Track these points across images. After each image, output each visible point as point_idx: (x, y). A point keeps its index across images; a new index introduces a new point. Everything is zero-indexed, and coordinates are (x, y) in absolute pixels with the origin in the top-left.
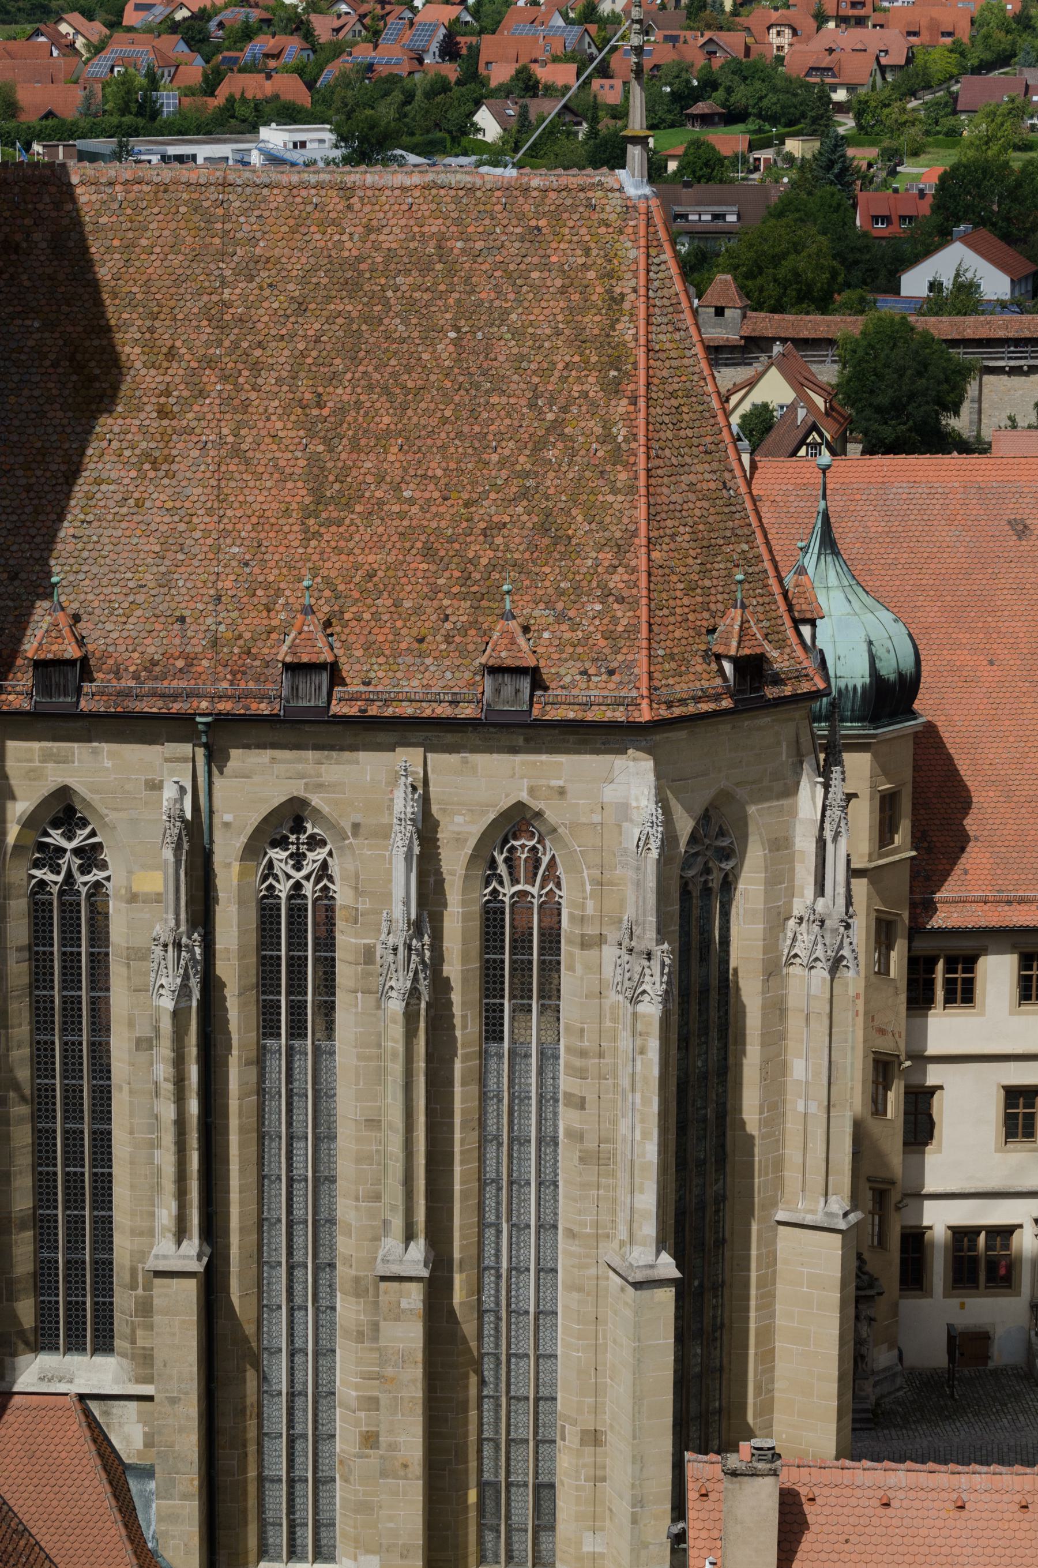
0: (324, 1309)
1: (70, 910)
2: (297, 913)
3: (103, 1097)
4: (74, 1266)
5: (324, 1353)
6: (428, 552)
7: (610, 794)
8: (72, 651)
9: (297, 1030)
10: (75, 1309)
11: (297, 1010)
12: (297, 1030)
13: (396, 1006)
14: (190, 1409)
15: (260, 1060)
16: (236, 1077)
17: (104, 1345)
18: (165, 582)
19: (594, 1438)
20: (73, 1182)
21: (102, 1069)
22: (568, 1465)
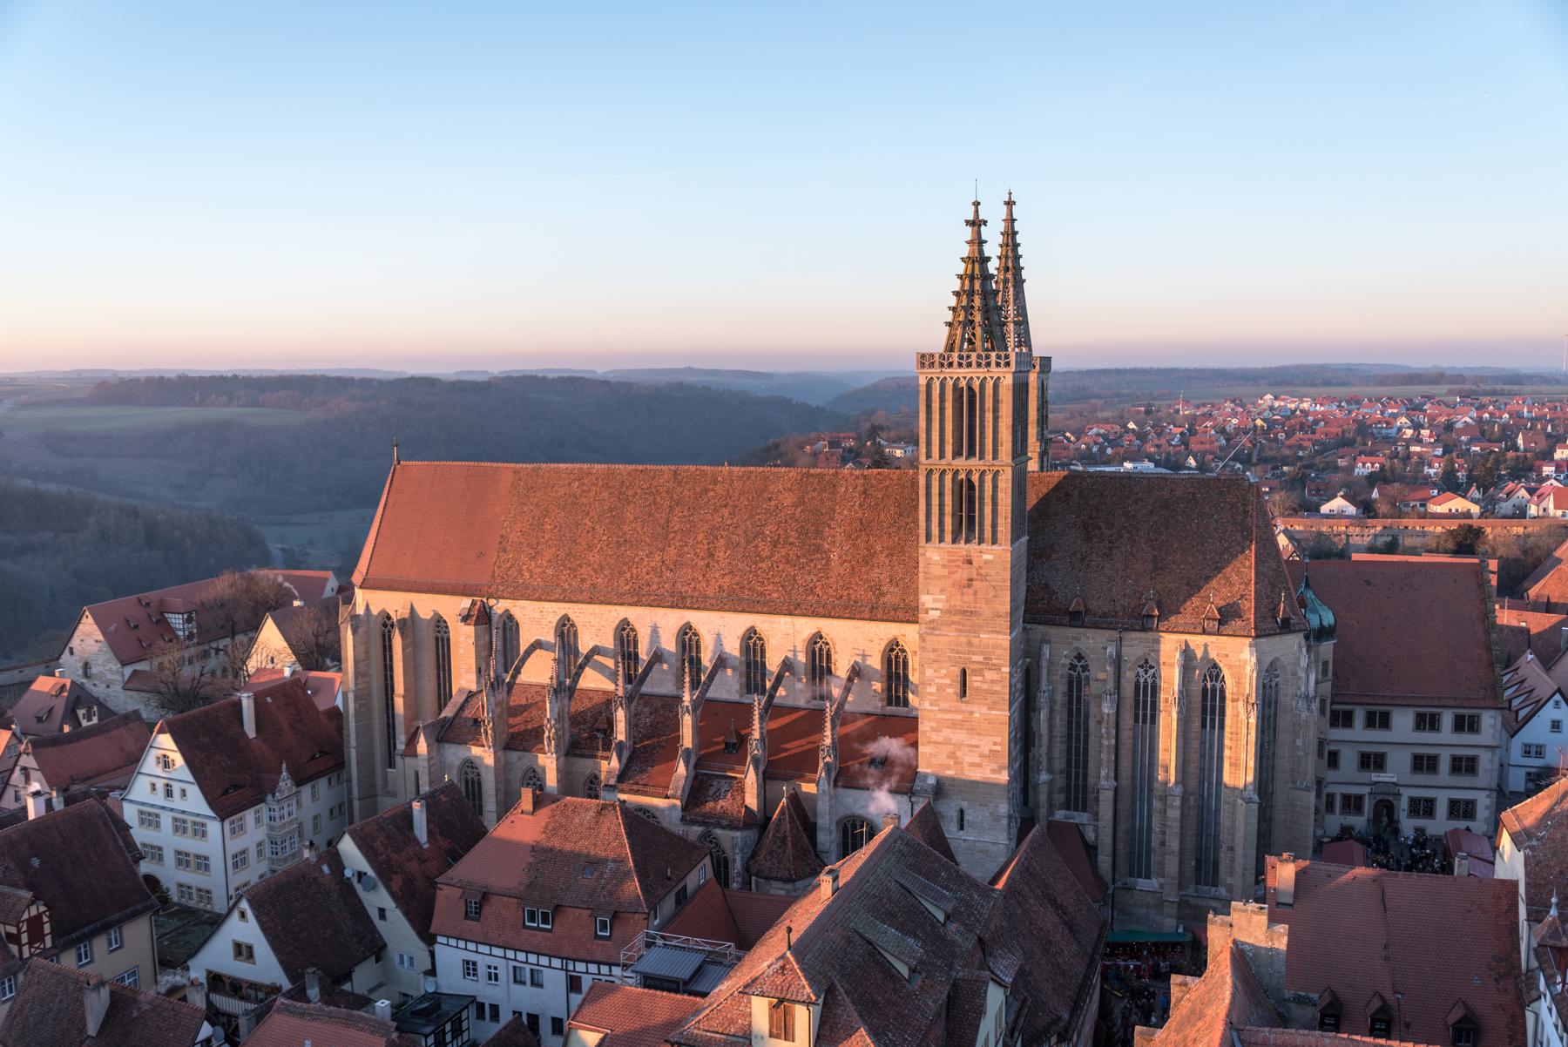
0: (1150, 804)
1: (1079, 683)
2: (1145, 687)
3: (1086, 737)
4: (1077, 786)
5: (1150, 816)
6: (1188, 584)
7: (1242, 657)
8: (1082, 609)
9: (1144, 721)
10: (1076, 798)
11: (1145, 715)
12: (1144, 721)
13: (1175, 715)
14: (1109, 830)
15: (1134, 729)
16: (1126, 734)
17: (1084, 810)
18: (1109, 590)
19: (1232, 849)
20: (1077, 761)
21: (1087, 730)
22: (1224, 855)
